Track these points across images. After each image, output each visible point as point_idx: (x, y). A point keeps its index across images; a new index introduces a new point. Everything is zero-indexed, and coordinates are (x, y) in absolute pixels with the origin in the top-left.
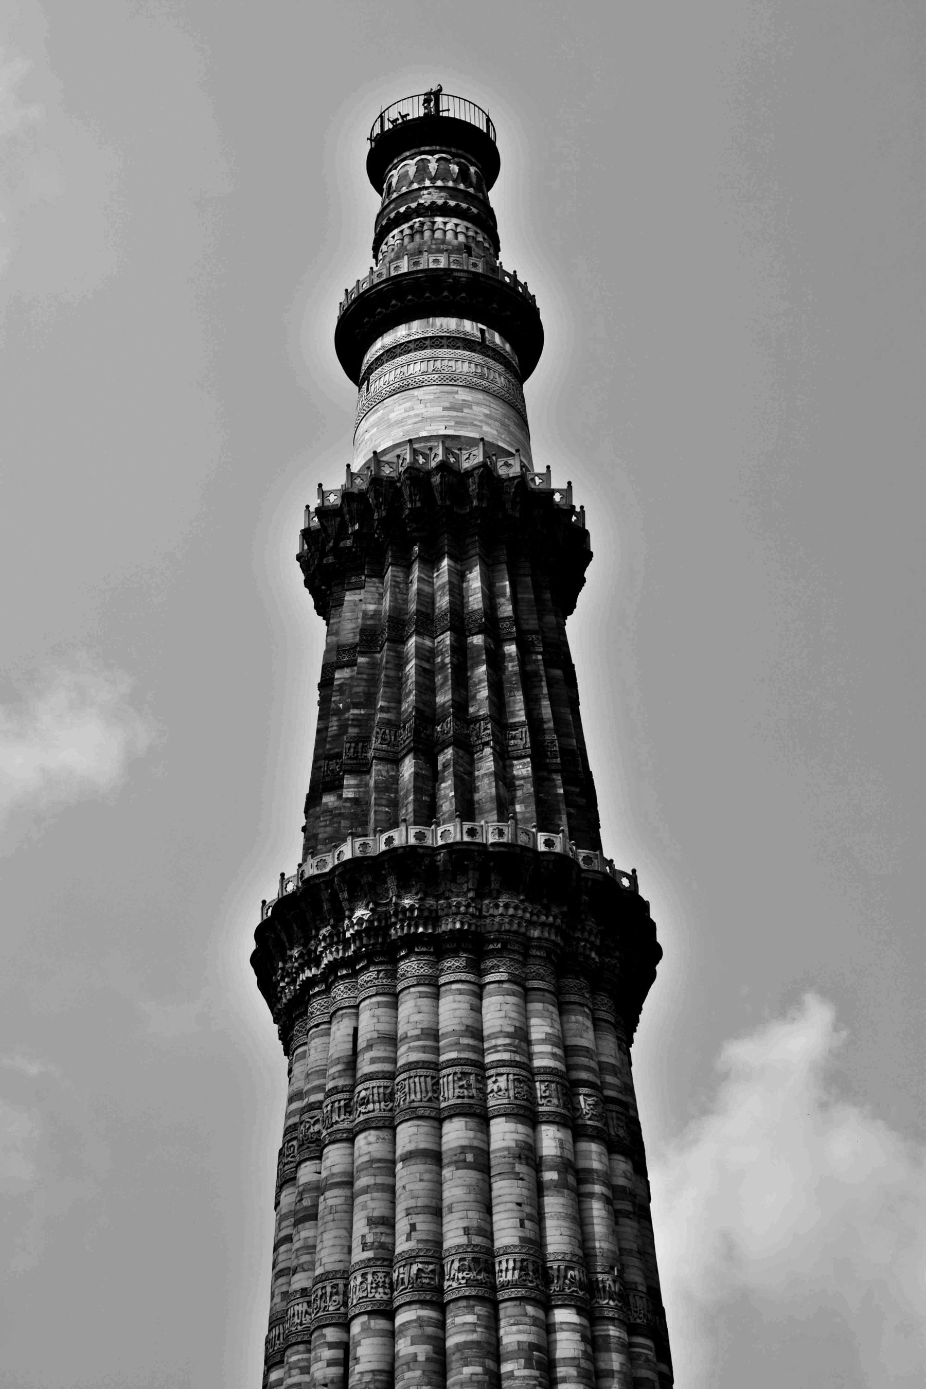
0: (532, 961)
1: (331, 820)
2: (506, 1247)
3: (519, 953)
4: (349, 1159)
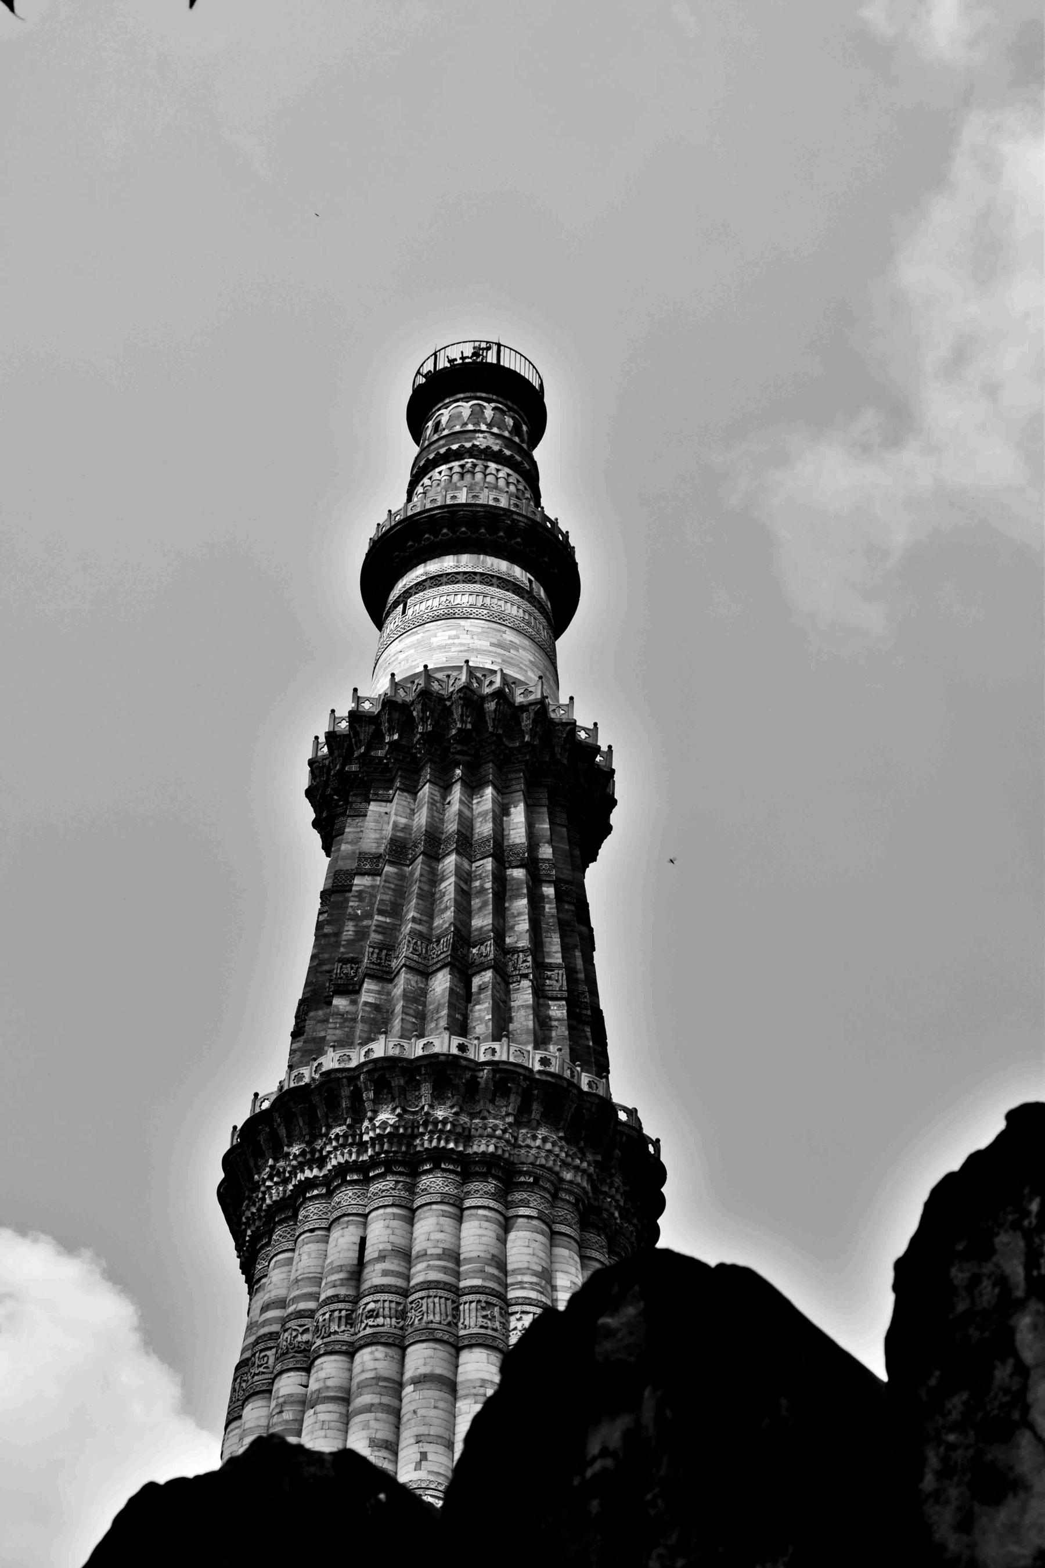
0: (560, 1204)
1: (340, 1023)
3: (549, 1192)
4: (347, 1374)
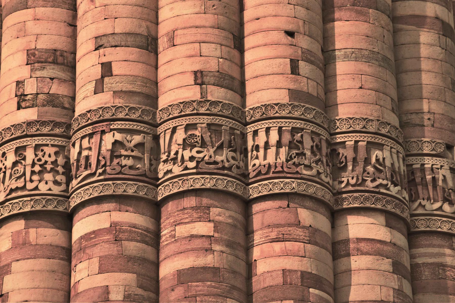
2: (266, 106)
